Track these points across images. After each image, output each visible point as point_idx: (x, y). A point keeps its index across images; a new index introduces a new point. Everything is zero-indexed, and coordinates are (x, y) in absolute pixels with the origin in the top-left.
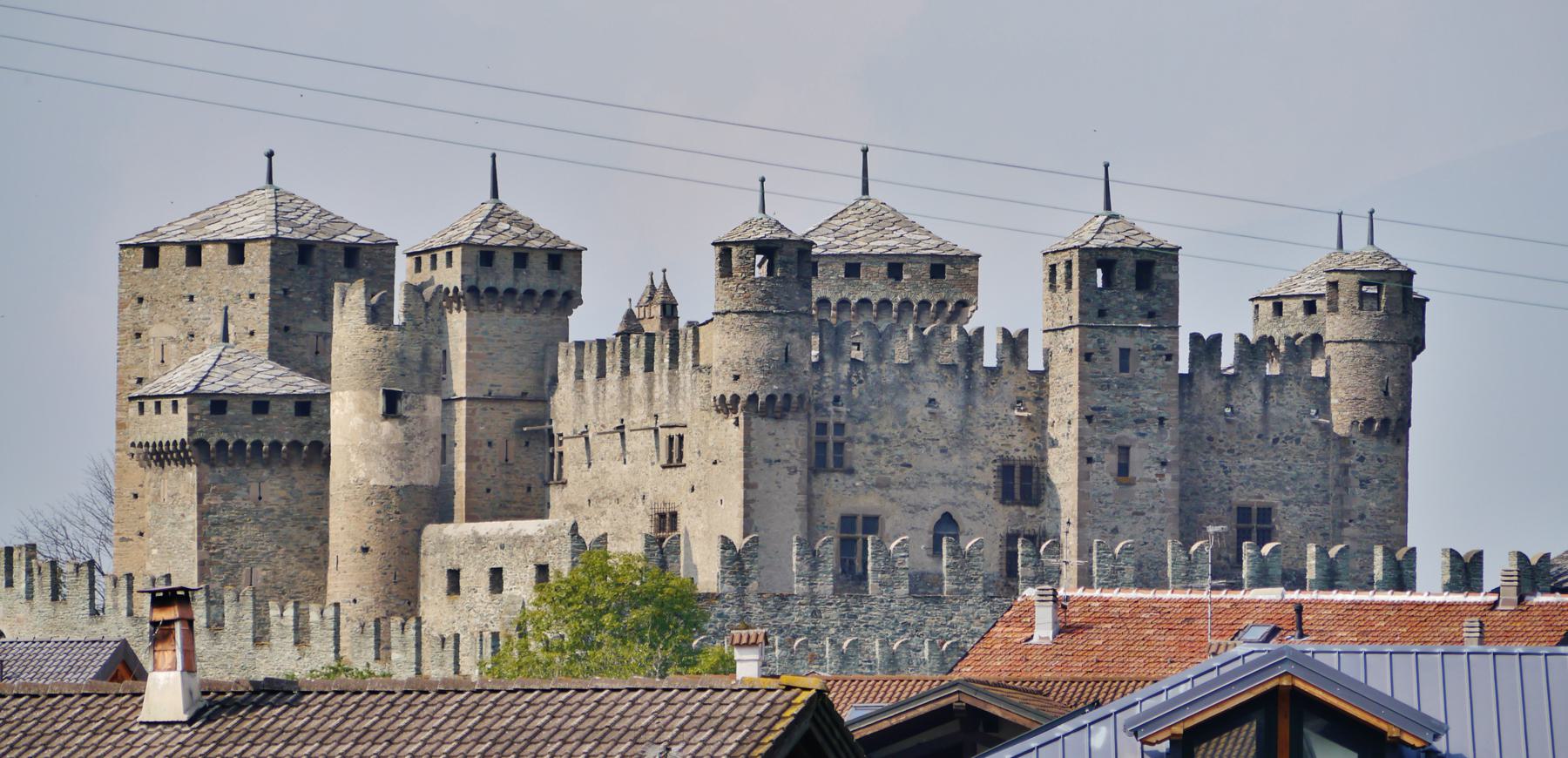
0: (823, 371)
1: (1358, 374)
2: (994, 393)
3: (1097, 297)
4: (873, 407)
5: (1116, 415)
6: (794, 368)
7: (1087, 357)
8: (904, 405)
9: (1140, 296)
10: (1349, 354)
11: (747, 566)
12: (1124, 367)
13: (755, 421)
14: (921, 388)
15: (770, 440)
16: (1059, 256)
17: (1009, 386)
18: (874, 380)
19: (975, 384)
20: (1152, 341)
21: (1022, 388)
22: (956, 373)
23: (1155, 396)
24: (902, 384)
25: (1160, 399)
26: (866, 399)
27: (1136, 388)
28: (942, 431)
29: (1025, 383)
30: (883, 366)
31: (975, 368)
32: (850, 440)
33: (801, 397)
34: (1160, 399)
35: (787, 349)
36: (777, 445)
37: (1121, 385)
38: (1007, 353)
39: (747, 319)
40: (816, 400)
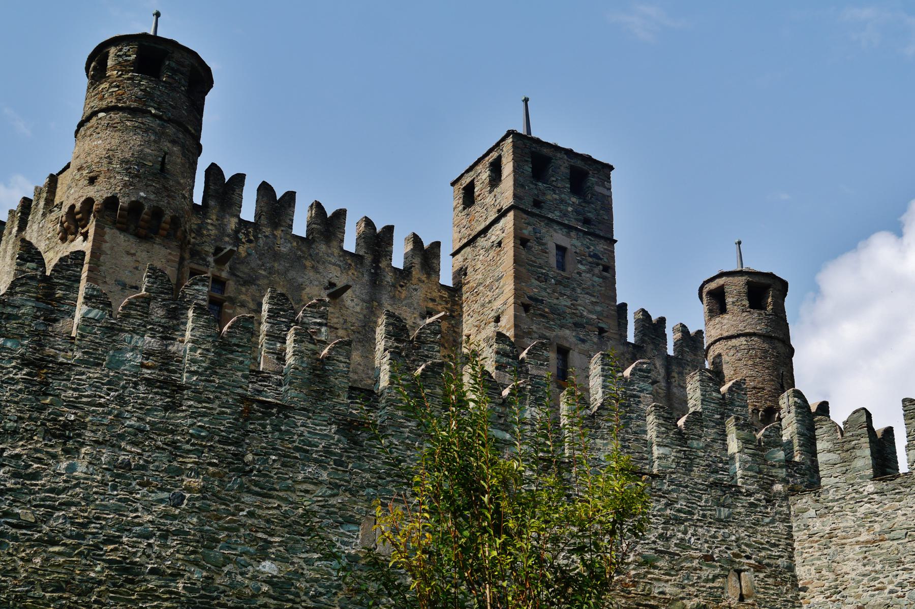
0: (206, 216)
1: (754, 365)
2: (403, 296)
3: (532, 186)
4: (263, 273)
5: (554, 310)
6: (171, 183)
7: (521, 242)
8: (300, 280)
9: (574, 200)
10: (742, 347)
11: (59, 293)
12: (561, 266)
13: (110, 233)
14: (321, 268)
15: (127, 260)
16: (479, 168)
17: (419, 293)
18: (266, 244)
19: (381, 281)
20: (589, 248)
21: (433, 300)
22: (362, 263)
23: (593, 303)
24: (299, 258)
25: (598, 309)
26: (255, 262)
27: (574, 289)
28: (341, 321)
29: (435, 294)
30: (278, 233)
31: (383, 265)
32: (232, 300)
33: (175, 221)
34: (598, 309)
35: (164, 158)
36: (136, 268)
37: (559, 283)
38: (417, 261)
39: (116, 117)
40: (194, 244)
